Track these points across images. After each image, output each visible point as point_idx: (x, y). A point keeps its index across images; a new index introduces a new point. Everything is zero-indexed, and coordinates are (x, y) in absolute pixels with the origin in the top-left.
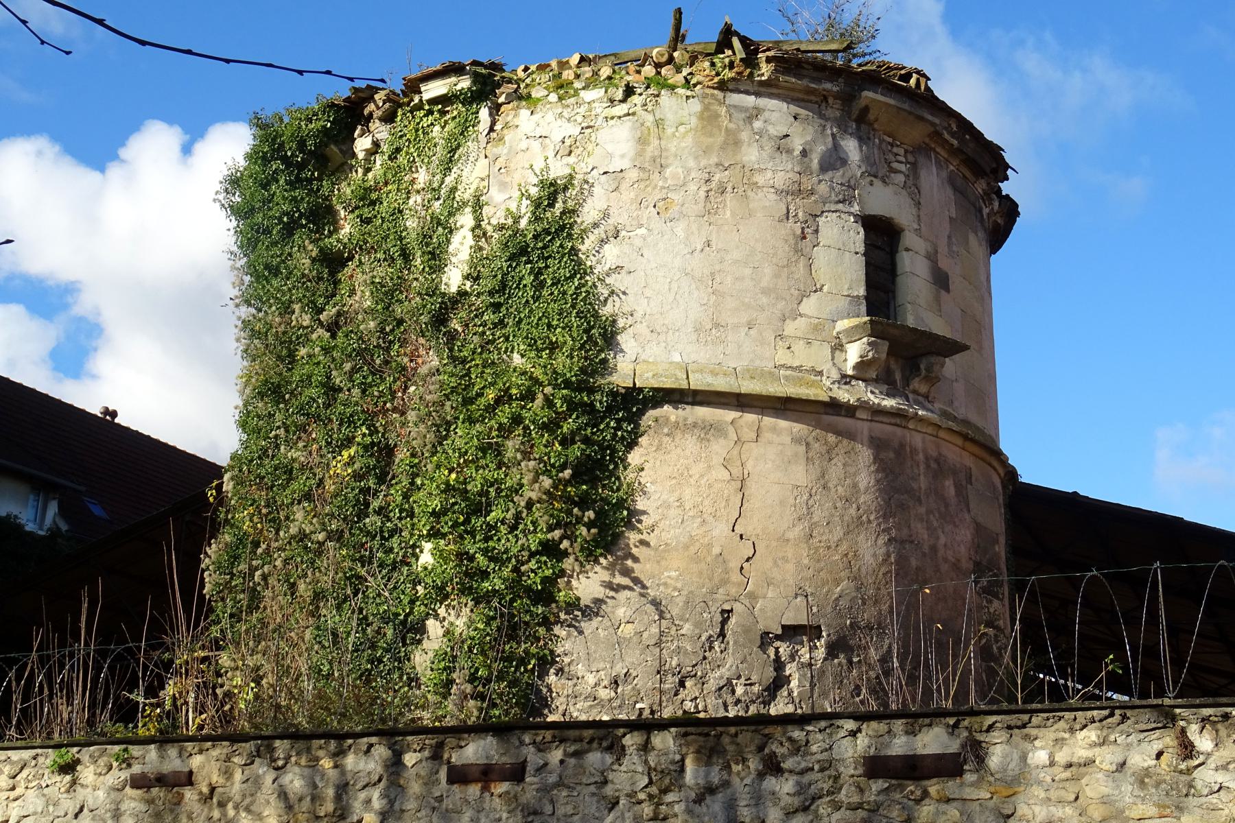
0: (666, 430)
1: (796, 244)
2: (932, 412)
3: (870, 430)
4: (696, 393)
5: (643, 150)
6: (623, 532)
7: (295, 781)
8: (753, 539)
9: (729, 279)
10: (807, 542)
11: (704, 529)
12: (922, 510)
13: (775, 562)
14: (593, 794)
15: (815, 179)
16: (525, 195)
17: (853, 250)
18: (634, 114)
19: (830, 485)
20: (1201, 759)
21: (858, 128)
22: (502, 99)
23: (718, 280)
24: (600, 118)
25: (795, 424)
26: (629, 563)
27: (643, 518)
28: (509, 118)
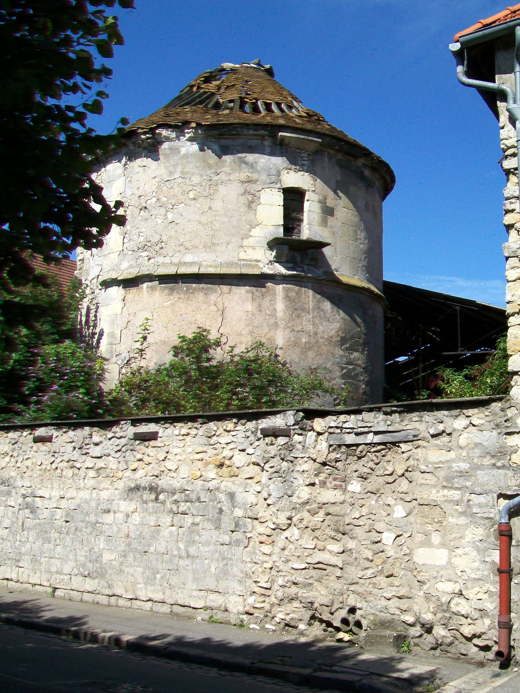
0: (191, 291)
19: (263, 310)
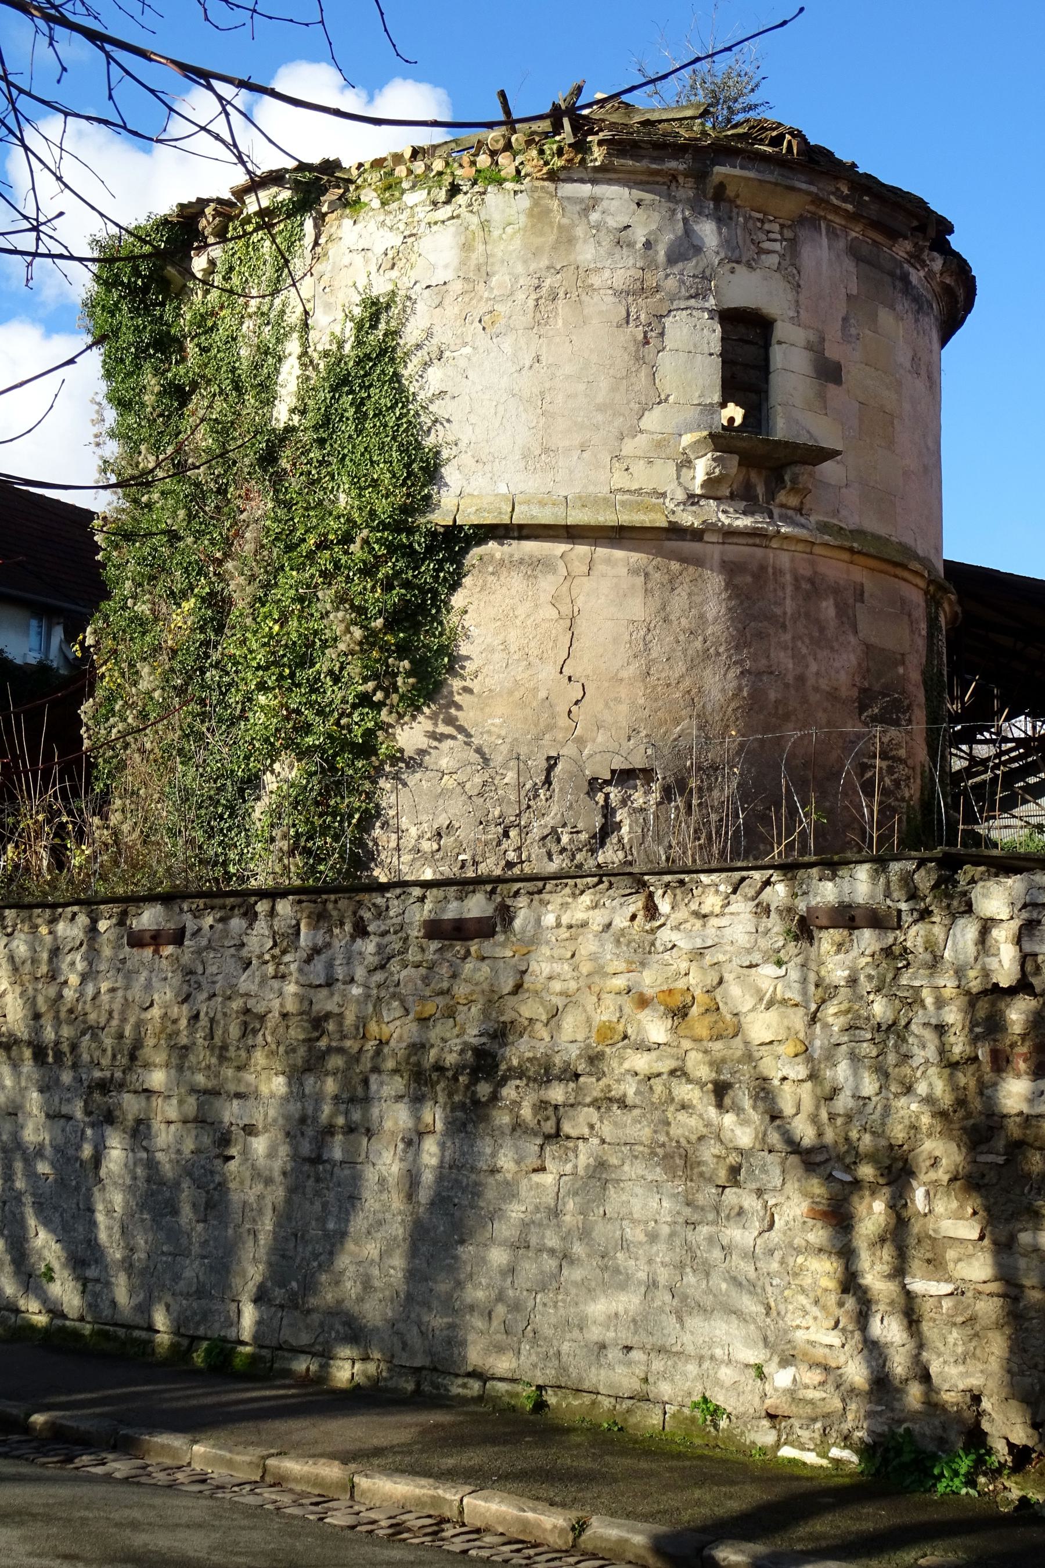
0: (491, 569)
1: (637, 351)
2: (803, 526)
3: (722, 553)
4: (521, 527)
5: (468, 258)
6: (446, 679)
7: (21, 947)
8: (583, 680)
9: (560, 399)
10: (643, 681)
11: (529, 672)
12: (787, 637)
13: (607, 704)
14: (233, 956)
15: (661, 274)
16: (349, 317)
17: (706, 351)
18: (458, 216)
19: (672, 617)
20: (662, 920)
21: (717, 208)
22: (325, 209)
23: (548, 399)
24: (423, 224)
25: (632, 554)
26: (453, 711)
27: (466, 664)
28: (333, 230)
